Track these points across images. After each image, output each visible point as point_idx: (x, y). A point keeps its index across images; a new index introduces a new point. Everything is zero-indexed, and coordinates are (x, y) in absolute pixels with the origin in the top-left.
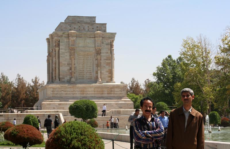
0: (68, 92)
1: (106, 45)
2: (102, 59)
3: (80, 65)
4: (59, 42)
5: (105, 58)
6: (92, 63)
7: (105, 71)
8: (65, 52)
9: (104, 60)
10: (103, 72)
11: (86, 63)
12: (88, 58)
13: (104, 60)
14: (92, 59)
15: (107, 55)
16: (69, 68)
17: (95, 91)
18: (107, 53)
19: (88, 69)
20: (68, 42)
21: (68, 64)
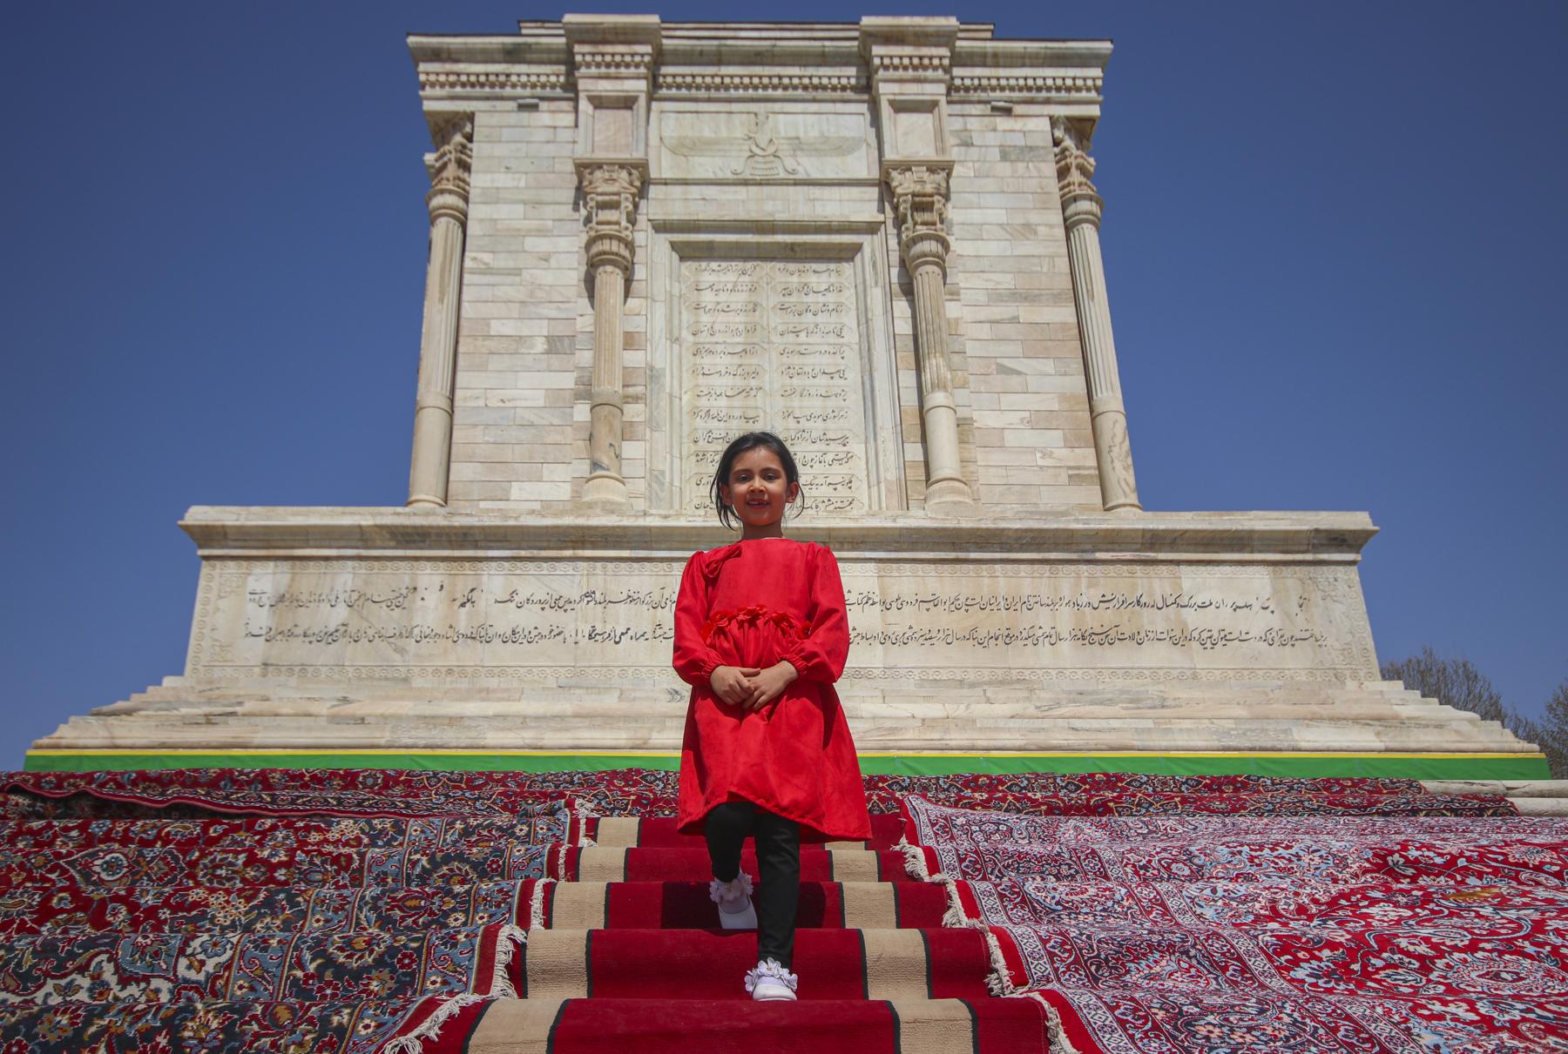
0: (505, 619)
1: (1004, 156)
2: (964, 295)
3: (707, 361)
4: (470, 138)
5: (1007, 282)
6: (851, 337)
7: (1014, 418)
8: (534, 224)
9: (996, 297)
10: (985, 419)
11: (776, 338)
12: (805, 288)
13: (996, 297)
14: (848, 297)
15: (1027, 248)
16: (568, 381)
17: (900, 603)
18: (1029, 229)
19: (816, 405)
20: (565, 135)
21: (555, 345)
